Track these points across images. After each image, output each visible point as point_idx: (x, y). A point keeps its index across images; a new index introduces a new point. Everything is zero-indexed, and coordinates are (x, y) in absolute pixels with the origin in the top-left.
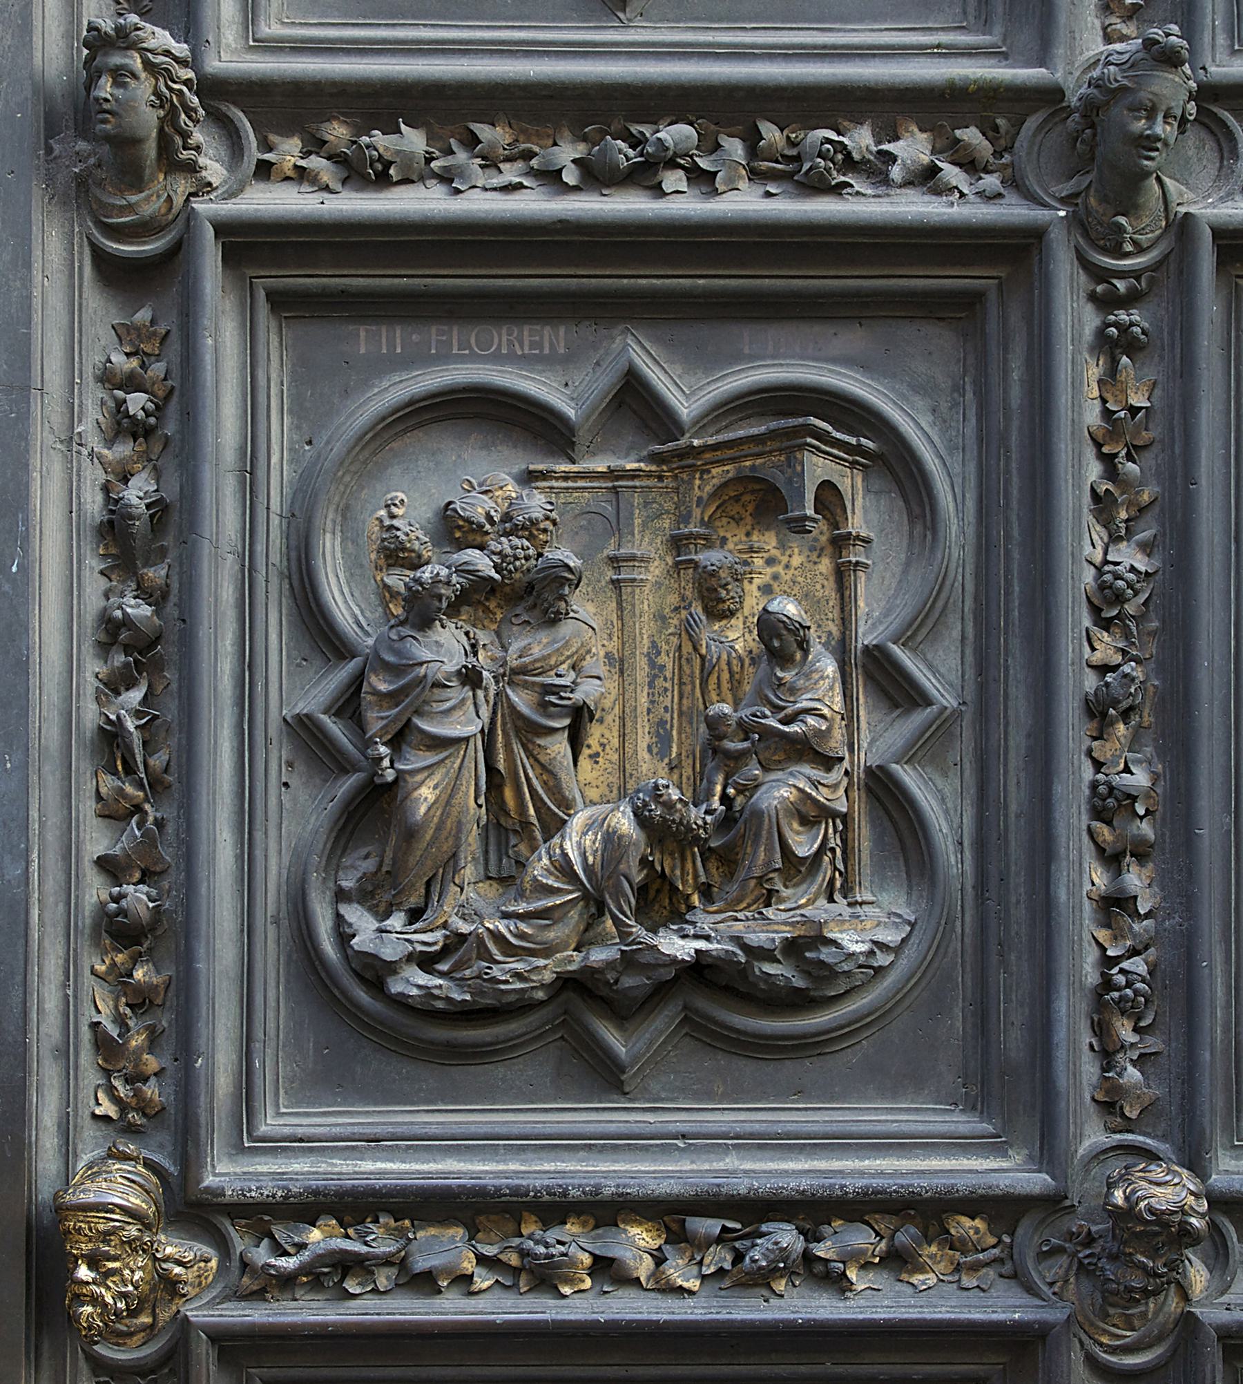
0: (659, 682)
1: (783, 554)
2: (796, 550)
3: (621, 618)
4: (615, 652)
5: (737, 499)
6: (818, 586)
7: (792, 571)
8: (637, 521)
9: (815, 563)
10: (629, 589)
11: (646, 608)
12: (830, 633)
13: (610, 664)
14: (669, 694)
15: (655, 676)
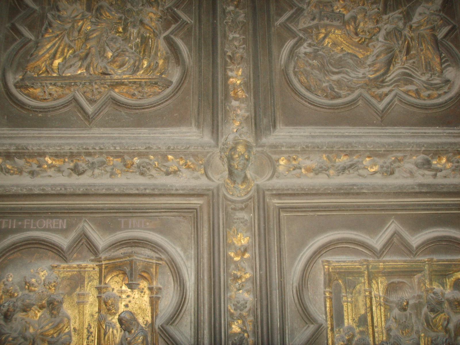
0: (91, 338)
1: (132, 294)
2: (137, 292)
3: (79, 315)
4: (76, 327)
5: (117, 276)
6: (144, 305)
7: (135, 299)
8: (86, 283)
9: (143, 297)
10: (82, 306)
11: (87, 312)
12: (147, 321)
13: (75, 332)
14: (93, 342)
15: (89, 336)
